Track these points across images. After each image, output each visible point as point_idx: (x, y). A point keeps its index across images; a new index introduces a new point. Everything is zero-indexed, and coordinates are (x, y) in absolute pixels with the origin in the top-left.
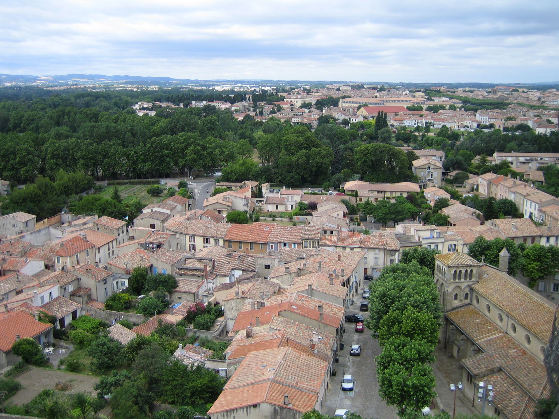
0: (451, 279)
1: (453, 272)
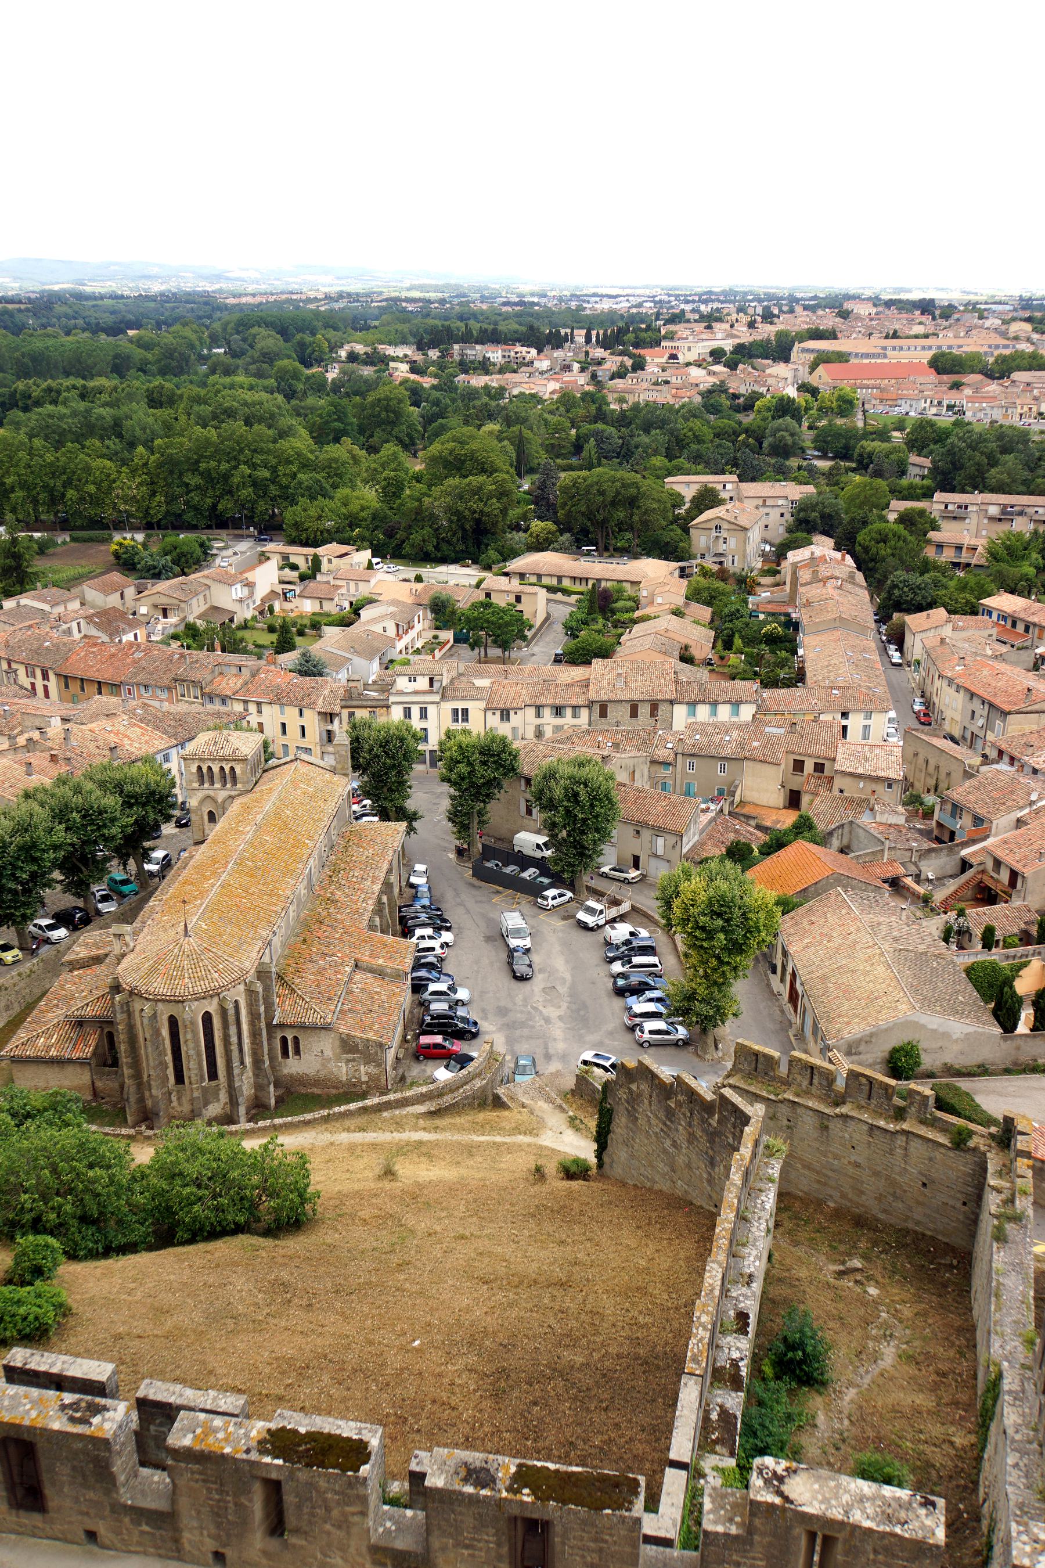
0: (192, 781)
1: (194, 769)
